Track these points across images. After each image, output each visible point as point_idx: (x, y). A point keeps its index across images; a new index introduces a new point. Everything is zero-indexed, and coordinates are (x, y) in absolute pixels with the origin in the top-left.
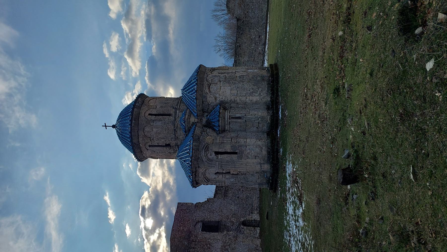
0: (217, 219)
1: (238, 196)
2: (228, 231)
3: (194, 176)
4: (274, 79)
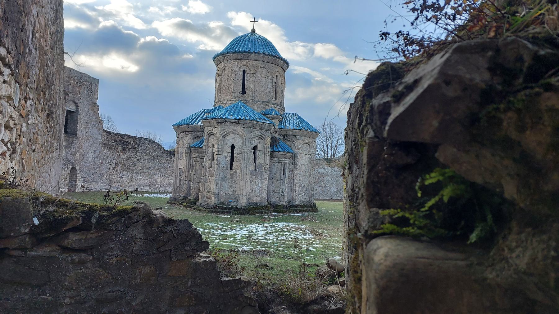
1: (104, 162)
2: (66, 147)
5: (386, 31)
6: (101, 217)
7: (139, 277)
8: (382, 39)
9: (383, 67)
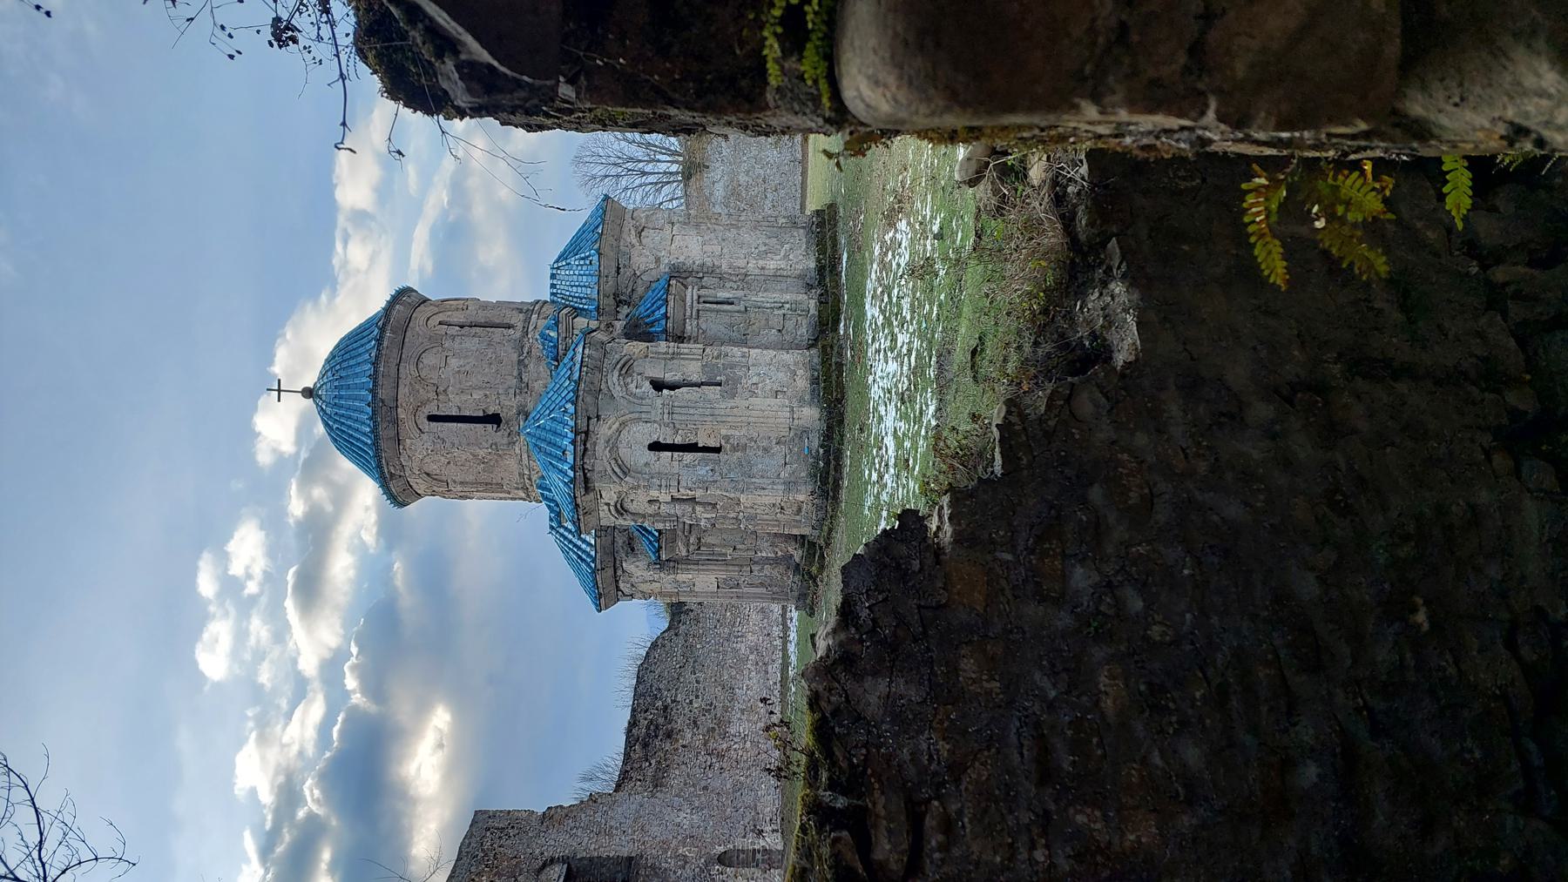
0: (625, 852)
1: (703, 783)
3: (580, 448)
4: (825, 230)
5: (269, 30)
6: (832, 785)
7: (986, 685)
8: (295, 41)
9: (370, 56)
